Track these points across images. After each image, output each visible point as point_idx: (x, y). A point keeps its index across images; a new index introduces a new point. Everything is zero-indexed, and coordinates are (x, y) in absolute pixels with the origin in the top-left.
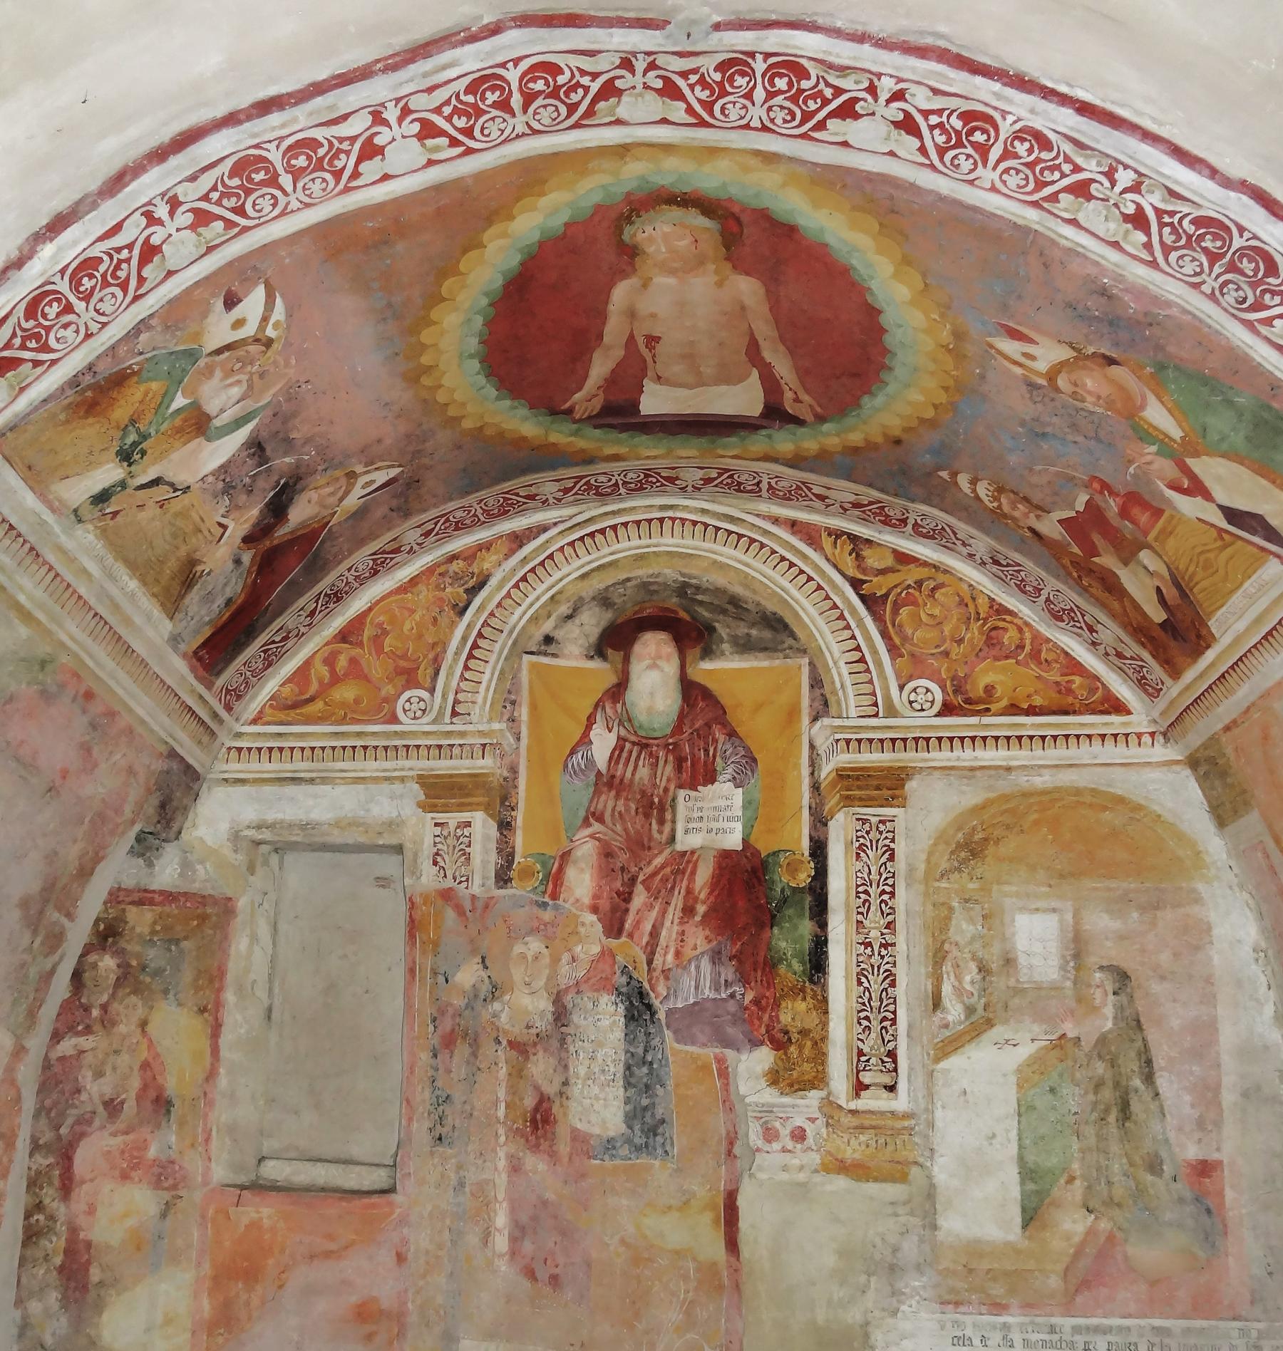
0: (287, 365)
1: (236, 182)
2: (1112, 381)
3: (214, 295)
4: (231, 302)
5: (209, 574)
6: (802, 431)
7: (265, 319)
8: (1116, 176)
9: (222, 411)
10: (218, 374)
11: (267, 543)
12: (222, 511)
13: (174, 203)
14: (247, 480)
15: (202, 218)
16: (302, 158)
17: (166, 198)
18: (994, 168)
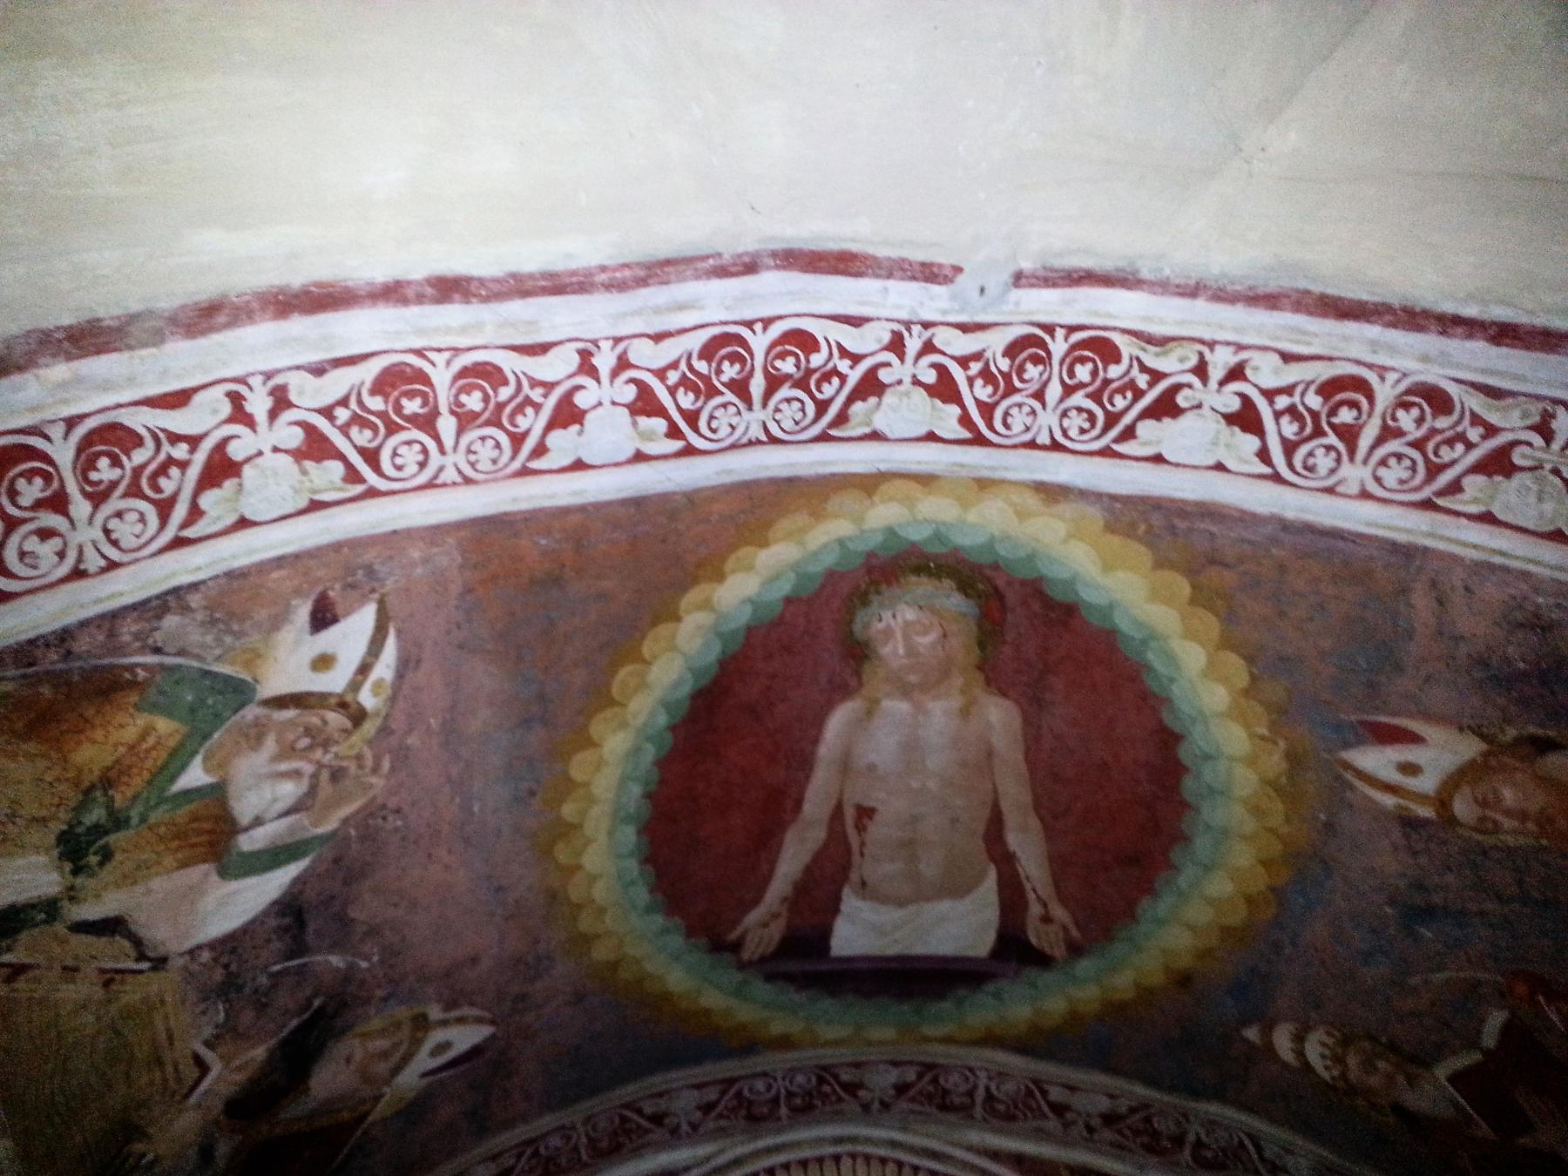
0: (375, 770)
1: (376, 403)
2: (1546, 782)
3: (298, 592)
4: (323, 618)
6: (1047, 978)
7: (364, 669)
8: (1554, 425)
9: (258, 822)
10: (270, 745)
12: (208, 1031)
13: (281, 401)
14: (263, 980)
15: (315, 447)
16: (477, 395)
17: (271, 383)
18: (1365, 462)
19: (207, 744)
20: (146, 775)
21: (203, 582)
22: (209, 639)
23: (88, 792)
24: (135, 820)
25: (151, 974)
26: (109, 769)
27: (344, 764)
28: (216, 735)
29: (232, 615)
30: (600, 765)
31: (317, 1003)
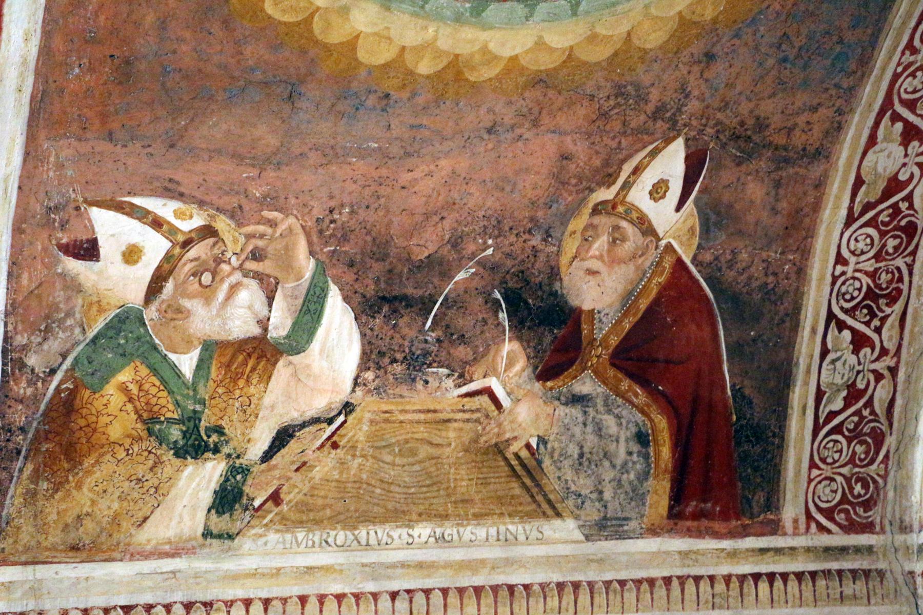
0: (273, 224)
5: (542, 440)
7: (157, 224)
9: (264, 324)
11: (599, 355)
12: (449, 383)
14: (432, 336)
19: (162, 348)
20: (165, 394)
21: (6, 332)
22: (61, 335)
23: (150, 432)
24: (198, 408)
25: (351, 418)
26: (140, 416)
27: (250, 248)
28: (157, 341)
29: (47, 317)
30: (384, 37)
31: (497, 295)
